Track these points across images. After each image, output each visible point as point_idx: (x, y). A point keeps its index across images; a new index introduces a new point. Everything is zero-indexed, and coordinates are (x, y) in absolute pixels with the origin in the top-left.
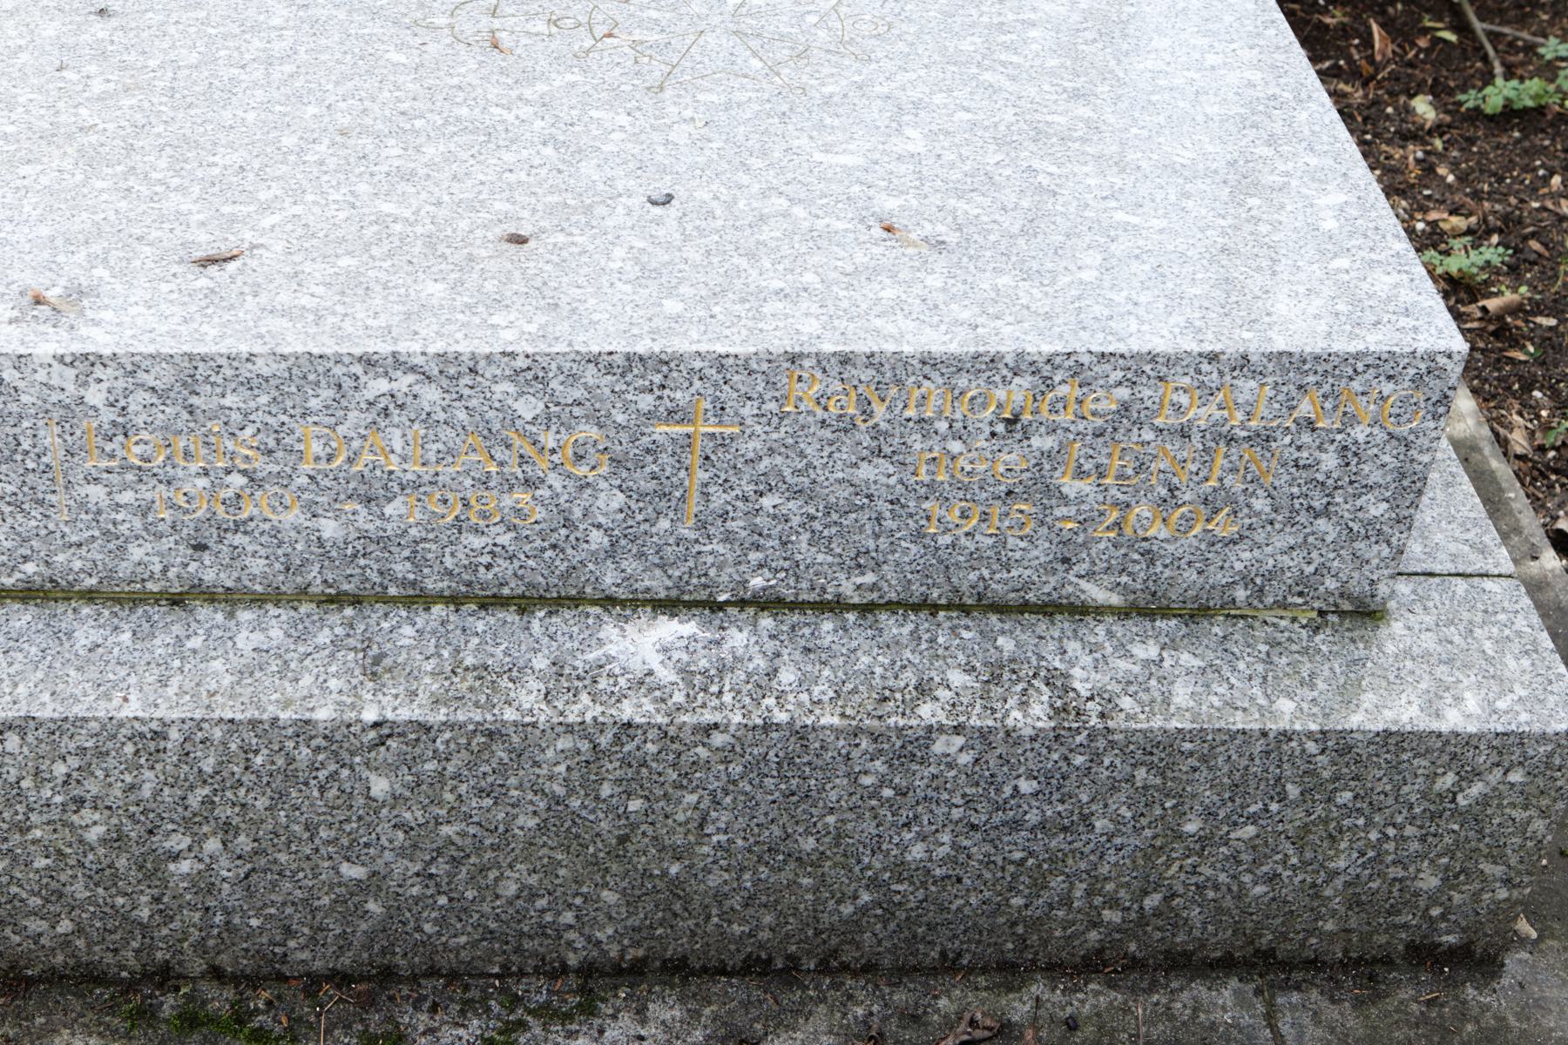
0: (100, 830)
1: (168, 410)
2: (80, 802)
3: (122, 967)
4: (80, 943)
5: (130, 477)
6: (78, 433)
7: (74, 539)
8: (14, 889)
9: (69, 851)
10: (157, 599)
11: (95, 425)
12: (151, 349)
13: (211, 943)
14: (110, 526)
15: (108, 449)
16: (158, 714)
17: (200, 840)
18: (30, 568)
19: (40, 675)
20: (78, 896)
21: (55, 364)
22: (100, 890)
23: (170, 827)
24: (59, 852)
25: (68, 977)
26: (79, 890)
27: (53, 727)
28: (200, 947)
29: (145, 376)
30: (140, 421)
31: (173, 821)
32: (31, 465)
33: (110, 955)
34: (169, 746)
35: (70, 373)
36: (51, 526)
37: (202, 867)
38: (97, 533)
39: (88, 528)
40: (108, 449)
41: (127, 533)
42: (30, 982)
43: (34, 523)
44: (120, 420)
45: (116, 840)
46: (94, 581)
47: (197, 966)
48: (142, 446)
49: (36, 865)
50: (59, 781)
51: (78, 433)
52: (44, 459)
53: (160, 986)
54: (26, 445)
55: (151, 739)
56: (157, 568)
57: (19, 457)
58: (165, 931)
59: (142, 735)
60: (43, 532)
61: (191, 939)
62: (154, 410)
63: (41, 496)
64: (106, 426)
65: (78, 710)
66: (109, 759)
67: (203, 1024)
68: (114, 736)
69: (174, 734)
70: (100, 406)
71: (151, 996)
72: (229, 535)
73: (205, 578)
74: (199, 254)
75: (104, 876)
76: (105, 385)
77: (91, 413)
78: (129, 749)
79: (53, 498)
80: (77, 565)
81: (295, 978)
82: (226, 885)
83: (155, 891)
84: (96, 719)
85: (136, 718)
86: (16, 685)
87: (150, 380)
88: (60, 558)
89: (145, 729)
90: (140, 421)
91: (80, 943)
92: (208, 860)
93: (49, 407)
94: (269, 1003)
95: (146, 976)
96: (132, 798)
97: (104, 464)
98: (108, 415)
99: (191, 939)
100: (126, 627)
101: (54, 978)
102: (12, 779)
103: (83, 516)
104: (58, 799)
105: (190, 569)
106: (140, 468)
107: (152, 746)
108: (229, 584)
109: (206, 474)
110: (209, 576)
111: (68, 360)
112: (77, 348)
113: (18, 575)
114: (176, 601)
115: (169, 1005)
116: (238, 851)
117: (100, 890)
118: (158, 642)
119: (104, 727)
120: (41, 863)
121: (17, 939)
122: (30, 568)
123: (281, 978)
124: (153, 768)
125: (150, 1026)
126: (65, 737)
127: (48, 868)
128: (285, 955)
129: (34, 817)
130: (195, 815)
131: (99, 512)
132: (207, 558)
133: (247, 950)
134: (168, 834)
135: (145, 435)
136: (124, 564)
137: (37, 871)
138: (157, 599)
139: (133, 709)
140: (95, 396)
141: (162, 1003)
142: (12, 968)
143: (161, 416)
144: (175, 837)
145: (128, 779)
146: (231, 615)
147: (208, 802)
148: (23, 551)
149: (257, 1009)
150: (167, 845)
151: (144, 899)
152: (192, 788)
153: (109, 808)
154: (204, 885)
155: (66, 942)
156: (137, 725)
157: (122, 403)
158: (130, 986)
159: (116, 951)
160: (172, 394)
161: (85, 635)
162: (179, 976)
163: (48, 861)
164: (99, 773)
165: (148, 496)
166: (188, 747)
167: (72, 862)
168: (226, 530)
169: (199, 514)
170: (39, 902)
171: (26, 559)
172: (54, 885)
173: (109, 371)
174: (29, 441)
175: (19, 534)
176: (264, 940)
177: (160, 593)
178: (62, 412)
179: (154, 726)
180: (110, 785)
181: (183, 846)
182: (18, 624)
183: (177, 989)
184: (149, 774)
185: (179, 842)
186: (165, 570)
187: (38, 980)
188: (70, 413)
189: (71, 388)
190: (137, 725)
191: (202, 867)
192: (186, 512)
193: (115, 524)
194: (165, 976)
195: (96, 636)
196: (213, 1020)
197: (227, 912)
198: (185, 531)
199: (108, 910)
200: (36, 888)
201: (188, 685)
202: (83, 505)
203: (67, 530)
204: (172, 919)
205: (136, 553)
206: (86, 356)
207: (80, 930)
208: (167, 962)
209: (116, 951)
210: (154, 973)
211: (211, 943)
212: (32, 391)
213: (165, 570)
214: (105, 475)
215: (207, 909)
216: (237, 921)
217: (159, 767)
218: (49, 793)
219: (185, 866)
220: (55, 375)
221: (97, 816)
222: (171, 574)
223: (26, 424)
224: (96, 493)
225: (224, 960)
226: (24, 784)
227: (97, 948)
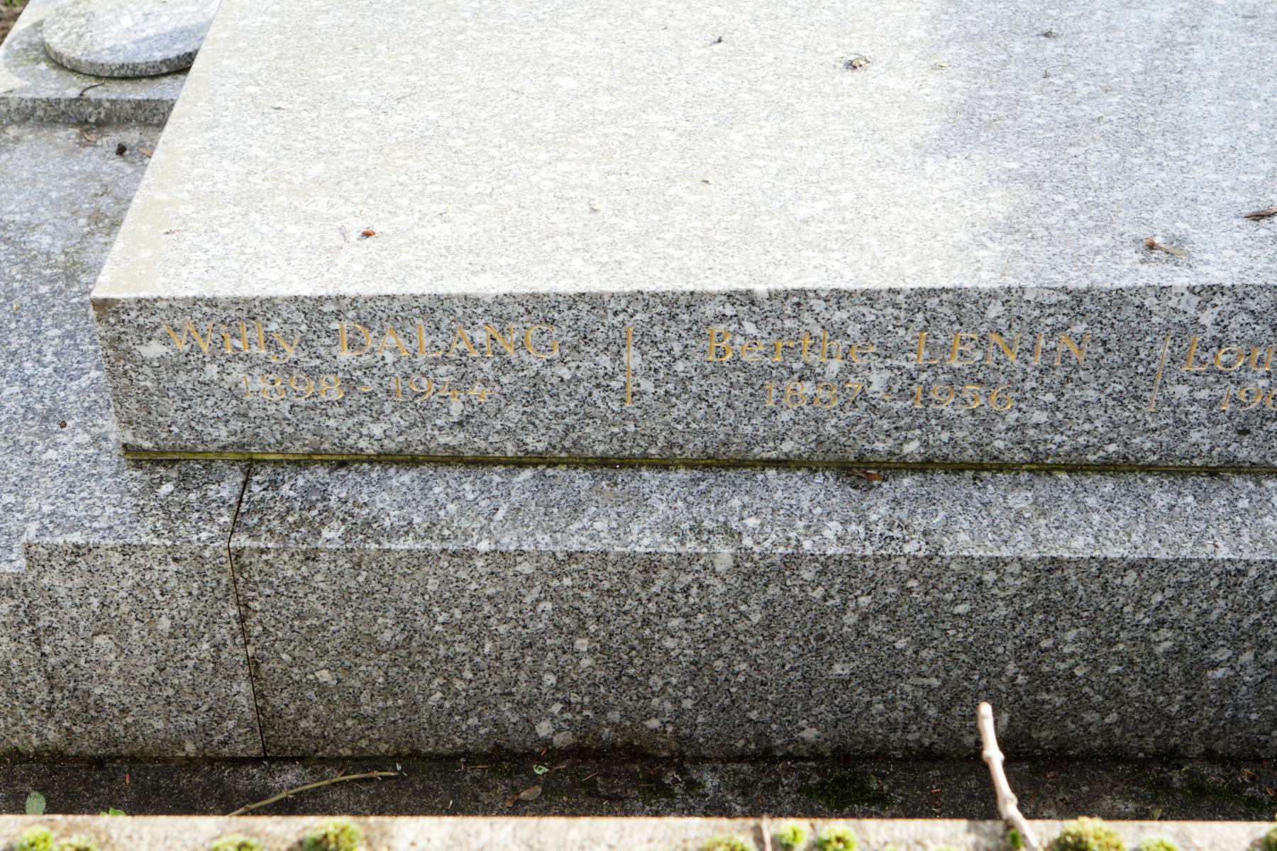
0: (1168, 644)
1: (1258, 328)
2: (1161, 623)
3: (1141, 749)
4: (1118, 731)
5: (1211, 379)
6: (1185, 345)
7: (1153, 425)
8: (1086, 689)
9: (1139, 660)
10: (1198, 471)
11: (1199, 339)
12: (1260, 282)
13: (1215, 732)
14: (1183, 417)
15: (1202, 358)
16: (1244, 557)
17: (1238, 653)
18: (1112, 448)
19: (1142, 528)
20: (1131, 695)
21: (1187, 293)
22: (1149, 691)
23: (1221, 643)
24: (1131, 662)
25: (1098, 757)
26: (1134, 691)
27: (1165, 565)
28: (1206, 735)
29: (1251, 302)
30: (1233, 337)
31: (1224, 639)
32: (1141, 369)
33: (1136, 740)
34: (1245, 581)
35: (1196, 300)
36: (1139, 416)
37: (1232, 673)
38: (1171, 421)
39: (1166, 417)
40: (1202, 358)
41: (1193, 421)
42: (1071, 759)
43: (1127, 414)
44: (1220, 335)
45: (1177, 653)
46: (1155, 458)
47: (1198, 748)
48: (1229, 355)
49: (1110, 671)
50: (1153, 607)
51: (1185, 345)
52: (1153, 366)
53: (1166, 764)
54: (1142, 356)
55: (1232, 575)
56: (1206, 448)
57: (1134, 364)
58: (1184, 722)
59: (1228, 573)
60: (1131, 421)
61: (1201, 729)
62: (1248, 327)
63: (1139, 393)
64: (1207, 340)
65: (1184, 553)
66: (1196, 591)
67: (1209, 793)
68: (1207, 573)
69: (1253, 572)
70: (1209, 325)
71: (1161, 772)
72: (1269, 423)
73: (1240, 455)
74: (1247, 211)
75: (1158, 681)
76: (1218, 309)
77: (1200, 330)
78: (1215, 583)
79: (1148, 395)
80: (1148, 445)
81: (1267, 759)
82: (1244, 688)
83: (1189, 692)
84: (1198, 560)
85: (1229, 560)
86: (1129, 535)
87: (1251, 304)
88: (1137, 440)
89: (1232, 568)
90: (1233, 337)
91: (1118, 731)
92: (1238, 668)
93: (1170, 326)
94: (1252, 778)
95: (1157, 757)
96: (1202, 620)
97: (1196, 369)
98: (1212, 331)
99: (1201, 729)
100: (1186, 492)
101: (1089, 757)
102: (1118, 605)
103: (1166, 409)
104: (1147, 621)
105: (1230, 449)
106: (1221, 372)
107: (1233, 580)
108: (1255, 460)
109: (1269, 377)
110: (1242, 454)
111: (1197, 290)
112: (1204, 281)
113: (1101, 453)
114: (1213, 473)
115: (1177, 778)
116: (1264, 662)
117: (1149, 691)
118: (1215, 502)
119: (1202, 567)
120: (1114, 669)
121: (1073, 726)
122: (1112, 448)
123: (1257, 760)
124: (1226, 597)
125: (1169, 794)
126: (1171, 575)
127: (1118, 673)
128: (1267, 741)
129: (1123, 635)
130: (1243, 634)
131: (1178, 406)
132: (1246, 440)
133: (1239, 738)
134: (1217, 648)
135: (1234, 347)
136: (1183, 445)
137: (1109, 675)
138: (1198, 471)
139: (1223, 553)
140: (1207, 318)
141: (1171, 778)
142: (1059, 749)
143: (1251, 332)
144: (1221, 651)
145: (1205, 606)
146: (1258, 484)
147: (1258, 624)
148: (1111, 435)
149: (1244, 783)
150: (1212, 657)
151: (1179, 697)
152: (1248, 614)
153: (1181, 628)
154: (1228, 688)
155: (1108, 730)
156: (1227, 565)
157: (1226, 323)
158: (1143, 765)
159: (1141, 737)
160: (1265, 316)
161: (1161, 499)
162: (1183, 757)
163: (1120, 668)
164: (1185, 602)
165: (1219, 393)
166: (1259, 582)
167: (1136, 669)
168: (1268, 419)
169: (1252, 407)
170: (1100, 698)
171: (1111, 441)
172: (1117, 686)
173: (1225, 298)
174: (1146, 352)
175: (1113, 423)
176: (1255, 730)
177: (1201, 467)
178: (1178, 330)
179: (1240, 566)
180: (1189, 610)
181: (1225, 657)
182: (1106, 490)
183: (1180, 767)
184: (1221, 602)
185: (1223, 654)
186: (1212, 449)
187: (1077, 758)
188: (1182, 330)
189: (1192, 312)
190: (1227, 565)
191: (1232, 673)
192: (1244, 405)
193: (1187, 414)
194: (1172, 757)
195: (1168, 499)
196: (1215, 791)
197: (1236, 708)
198: (1238, 419)
199: (1149, 706)
200: (1102, 688)
201: (1257, 536)
202: (1168, 401)
203: (1150, 419)
204: (1193, 713)
205: (1195, 436)
206: (1211, 287)
207: (1122, 721)
208: (1176, 745)
209: (1141, 737)
210: (1163, 755)
211: (1215, 732)
212: (1162, 314)
213: (1212, 449)
214: (1193, 377)
215: (1223, 706)
216: (1241, 715)
217: (1231, 597)
218: (1142, 616)
219: (1219, 673)
220: (1183, 302)
221: (1170, 634)
222: (1214, 453)
223: (1149, 339)
224: (1182, 391)
225: (1219, 746)
226: (1126, 609)
227: (1128, 735)
